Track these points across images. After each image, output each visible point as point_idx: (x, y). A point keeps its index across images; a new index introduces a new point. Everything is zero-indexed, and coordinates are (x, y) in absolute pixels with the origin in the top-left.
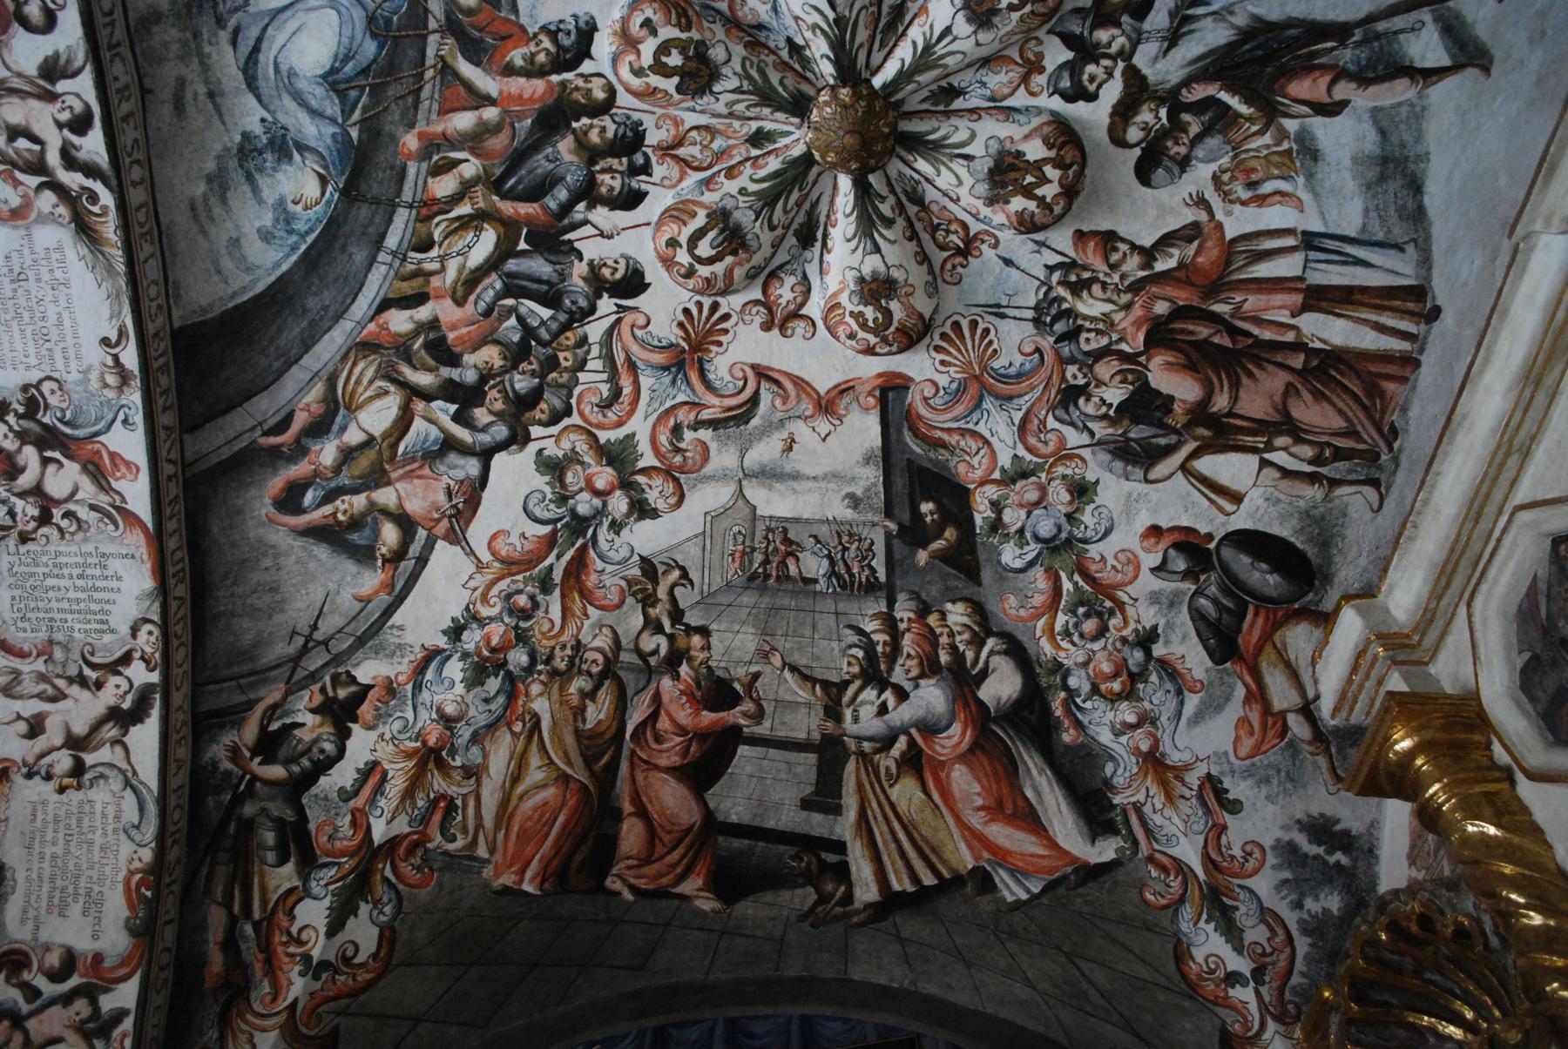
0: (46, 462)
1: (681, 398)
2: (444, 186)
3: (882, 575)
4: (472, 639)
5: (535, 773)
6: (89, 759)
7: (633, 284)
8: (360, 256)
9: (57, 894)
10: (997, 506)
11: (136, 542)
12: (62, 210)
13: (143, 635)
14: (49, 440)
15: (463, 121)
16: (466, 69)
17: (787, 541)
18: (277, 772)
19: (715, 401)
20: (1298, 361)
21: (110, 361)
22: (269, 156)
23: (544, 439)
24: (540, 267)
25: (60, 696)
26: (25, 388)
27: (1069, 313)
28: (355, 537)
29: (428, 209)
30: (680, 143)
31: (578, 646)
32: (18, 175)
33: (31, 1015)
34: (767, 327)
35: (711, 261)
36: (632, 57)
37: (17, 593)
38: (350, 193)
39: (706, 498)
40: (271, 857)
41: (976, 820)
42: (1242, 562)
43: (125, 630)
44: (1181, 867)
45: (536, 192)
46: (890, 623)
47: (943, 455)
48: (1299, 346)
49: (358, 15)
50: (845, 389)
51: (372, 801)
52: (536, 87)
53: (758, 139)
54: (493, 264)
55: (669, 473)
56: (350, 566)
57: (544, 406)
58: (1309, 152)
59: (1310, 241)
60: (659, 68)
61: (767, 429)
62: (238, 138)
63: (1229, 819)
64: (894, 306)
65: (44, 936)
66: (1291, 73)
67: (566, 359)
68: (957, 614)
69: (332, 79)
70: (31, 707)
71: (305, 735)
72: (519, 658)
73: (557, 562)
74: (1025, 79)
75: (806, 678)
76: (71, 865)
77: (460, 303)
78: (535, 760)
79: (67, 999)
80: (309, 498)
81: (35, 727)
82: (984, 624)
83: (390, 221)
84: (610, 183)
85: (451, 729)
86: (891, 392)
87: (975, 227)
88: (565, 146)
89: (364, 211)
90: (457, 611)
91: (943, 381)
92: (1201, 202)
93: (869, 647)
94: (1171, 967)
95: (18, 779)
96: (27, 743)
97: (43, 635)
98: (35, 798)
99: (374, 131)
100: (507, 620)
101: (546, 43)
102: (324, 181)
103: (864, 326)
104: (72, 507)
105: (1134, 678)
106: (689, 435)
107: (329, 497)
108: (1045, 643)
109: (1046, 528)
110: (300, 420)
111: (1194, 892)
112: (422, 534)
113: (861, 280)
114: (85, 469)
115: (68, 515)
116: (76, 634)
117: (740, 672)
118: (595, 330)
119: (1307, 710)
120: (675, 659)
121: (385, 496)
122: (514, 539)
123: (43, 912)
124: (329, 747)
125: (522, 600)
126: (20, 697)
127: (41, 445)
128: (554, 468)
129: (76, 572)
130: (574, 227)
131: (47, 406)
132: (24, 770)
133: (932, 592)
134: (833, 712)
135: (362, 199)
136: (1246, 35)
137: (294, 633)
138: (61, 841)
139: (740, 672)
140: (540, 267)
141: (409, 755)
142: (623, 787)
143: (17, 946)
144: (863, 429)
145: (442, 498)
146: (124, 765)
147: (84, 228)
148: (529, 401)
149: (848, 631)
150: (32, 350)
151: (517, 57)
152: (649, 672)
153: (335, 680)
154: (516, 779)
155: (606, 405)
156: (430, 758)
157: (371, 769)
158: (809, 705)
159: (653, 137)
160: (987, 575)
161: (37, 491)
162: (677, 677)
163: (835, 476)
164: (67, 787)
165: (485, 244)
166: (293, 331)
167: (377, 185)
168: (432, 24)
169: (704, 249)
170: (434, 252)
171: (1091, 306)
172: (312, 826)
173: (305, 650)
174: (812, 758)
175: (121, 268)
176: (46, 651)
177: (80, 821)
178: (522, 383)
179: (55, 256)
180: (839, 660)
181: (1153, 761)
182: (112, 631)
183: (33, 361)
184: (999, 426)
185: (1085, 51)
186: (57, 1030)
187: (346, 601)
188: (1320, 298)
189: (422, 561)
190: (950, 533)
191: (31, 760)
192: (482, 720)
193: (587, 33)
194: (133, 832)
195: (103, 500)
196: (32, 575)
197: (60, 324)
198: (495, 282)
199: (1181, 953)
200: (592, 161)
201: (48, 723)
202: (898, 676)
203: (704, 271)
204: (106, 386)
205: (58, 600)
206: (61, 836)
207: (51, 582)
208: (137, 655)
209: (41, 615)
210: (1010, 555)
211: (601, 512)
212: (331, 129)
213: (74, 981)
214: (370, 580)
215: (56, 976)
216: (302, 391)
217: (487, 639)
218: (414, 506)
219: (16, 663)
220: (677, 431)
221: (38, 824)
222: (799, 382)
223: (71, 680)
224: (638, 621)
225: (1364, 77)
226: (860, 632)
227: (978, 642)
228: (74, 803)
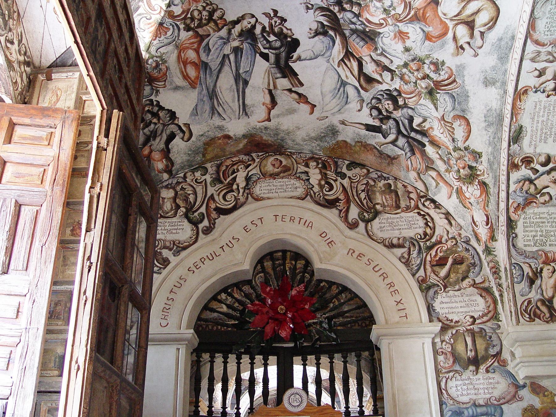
9: (543, 135)
33: (536, 179)
65: (538, 151)
70: (540, 66)
76: (549, 124)
79: (549, 172)
81: (541, 73)
95: (531, 93)
98: (537, 100)
123: (538, 142)
126: (538, 62)
132: (534, 90)
138: (546, 115)
143: (528, 155)
164: (550, 95)
186: (546, 184)
191: (537, 86)
201: (547, 71)
206: (546, 114)
213: (551, 165)
215: (544, 165)
219: (540, 48)
221: (537, 110)
228: (553, 101)
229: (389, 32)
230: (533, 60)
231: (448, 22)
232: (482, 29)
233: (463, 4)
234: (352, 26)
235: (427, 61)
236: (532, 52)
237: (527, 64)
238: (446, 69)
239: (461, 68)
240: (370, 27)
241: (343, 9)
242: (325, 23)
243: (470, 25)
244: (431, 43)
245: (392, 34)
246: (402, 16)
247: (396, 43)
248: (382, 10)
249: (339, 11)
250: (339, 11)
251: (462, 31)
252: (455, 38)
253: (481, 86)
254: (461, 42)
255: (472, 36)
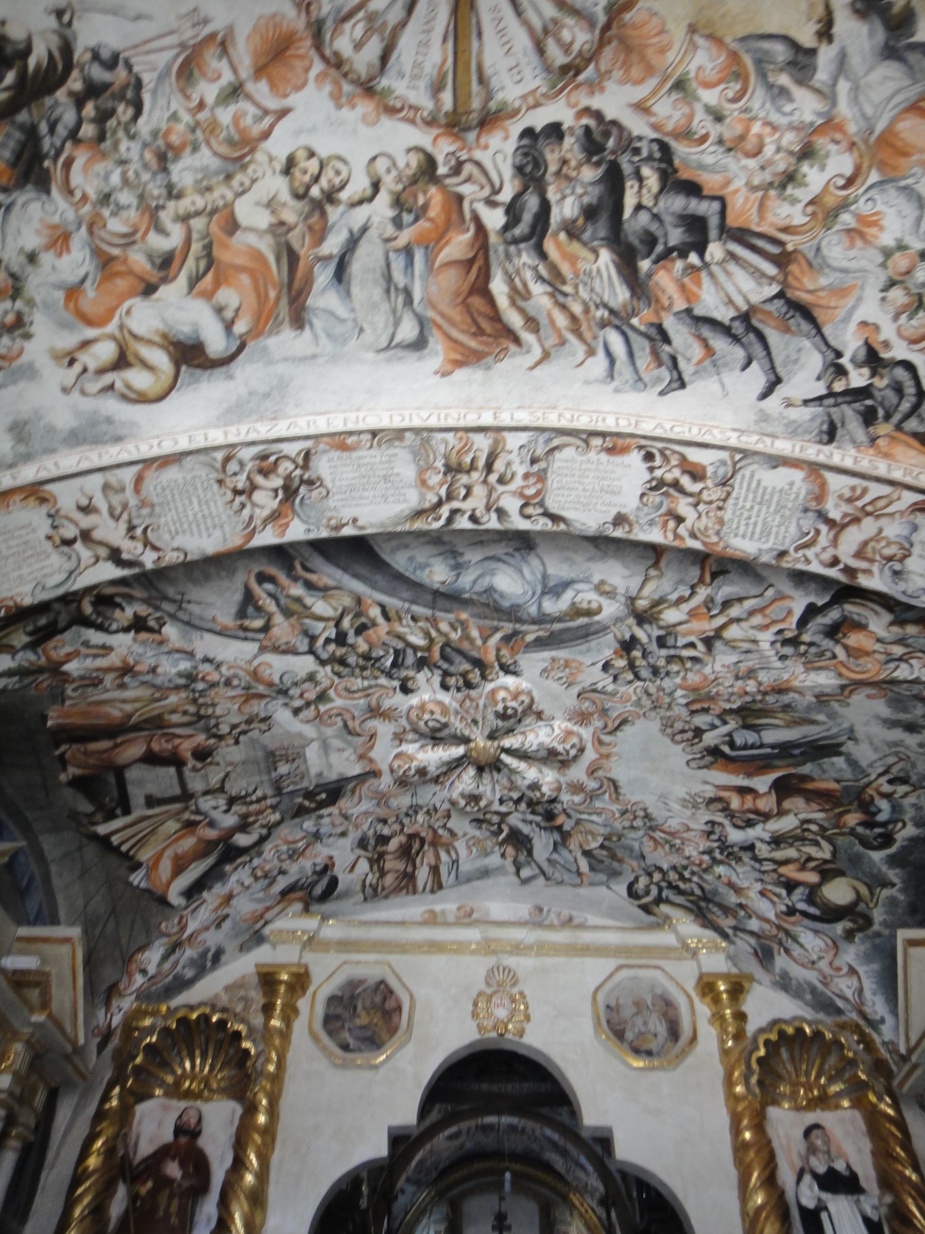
0: (276, 491)
1: (356, 714)
2: (444, 627)
3: (285, 791)
4: (206, 668)
5: (128, 708)
6: (78, 546)
7: (406, 689)
8: (406, 595)
10: (330, 815)
11: (235, 541)
12: (427, 505)
13: (175, 554)
14: (289, 492)
15: (475, 633)
16: (498, 636)
17: (294, 760)
18: (88, 609)
19: (357, 723)
20: (410, 869)
21: (344, 521)
22: (452, 562)
23: (325, 674)
24: (410, 659)
25: (117, 519)
26: (319, 479)
27: (416, 813)
28: (250, 610)
29: (434, 622)
30: (472, 700)
31: (214, 705)
32: (445, 487)
34: (395, 734)
35: (426, 723)
36: (509, 698)
37: (181, 481)
38: (436, 594)
39: (309, 731)
40: (30, 628)
41: (169, 853)
42: (325, 881)
43: (176, 544)
44: (183, 928)
45: (444, 656)
46: (264, 798)
47: (348, 794)
48: (415, 868)
49: (521, 601)
50: (371, 761)
51: (87, 656)
52: (491, 657)
53: (475, 722)
54: (409, 644)
55: (318, 715)
56: (233, 610)
57: (341, 669)
58: (487, 855)
59: (455, 862)
60: (506, 708)
61: (346, 741)
62: (461, 550)
63: (213, 928)
64: (417, 777)
66: (515, 847)
67: (367, 673)
68: (276, 817)
69: (490, 590)
70: (103, 506)
71: (118, 613)
72: (200, 686)
73: (261, 689)
74: (505, 788)
75: (223, 781)
77: (388, 633)
78: (137, 705)
80: (269, 586)
81: (86, 510)
82: (271, 828)
83: (425, 606)
84: (452, 681)
85: (148, 672)
86: (375, 774)
87: (448, 784)
88: (466, 666)
89: (429, 597)
90: (219, 658)
91: (382, 786)
92: (465, 835)
93: (247, 795)
94: (133, 950)
95: (44, 509)
96: (74, 507)
97: (155, 500)
99: (466, 603)
100: (223, 679)
101: (510, 662)
102: (444, 583)
103: (405, 772)
104: (249, 506)
105: (266, 876)
106: (339, 719)
107: (272, 595)
108: (270, 847)
109: (323, 830)
110: (313, 577)
111: (174, 938)
112: (261, 636)
113: (425, 768)
114: (274, 512)
115: (243, 506)
116: (163, 520)
117: (218, 759)
118: (383, 681)
119: (266, 923)
120: (221, 738)
121: (278, 619)
122: (268, 672)
124: (114, 626)
125: (235, 682)
127: (286, 488)
128: (311, 678)
129: (206, 512)
130: (431, 670)
131: (311, 491)
132: (53, 512)
133: (283, 807)
134: (206, 793)
135: (435, 598)
136: (527, 837)
137: (183, 595)
139: (218, 759)
140: (410, 659)
141: (124, 661)
142: (133, 735)
144: (356, 769)
145: (284, 640)
146: (82, 566)
147: (418, 513)
148: (342, 662)
149: (253, 788)
150: (344, 483)
151: (505, 652)
152: (207, 730)
153: (158, 619)
154: (124, 701)
155: (347, 689)
156: (126, 670)
157: (107, 649)
158: (208, 784)
159: (473, 693)
160: (297, 820)
161: (253, 487)
162: (207, 739)
163: (330, 766)
165: (417, 640)
166: (363, 571)
167: (441, 602)
168: (517, 626)
169: (431, 724)
170: (411, 623)
171: (420, 818)
172: (59, 637)
173: (173, 601)
174: (177, 791)
175: (399, 529)
176: (143, 504)
177: (32, 556)
178: (352, 660)
179: (402, 498)
180: (235, 787)
181: (230, 897)
182: (173, 538)
183: (337, 483)
184: (365, 806)
185: (518, 802)
187: (210, 613)
188: (435, 870)
189: (246, 639)
190: (313, 805)
191: (62, 513)
192: (158, 681)
193: (515, 673)
194: (39, 588)
195: (257, 522)
196: (196, 488)
197: (362, 498)
198: (400, 645)
199: (142, 948)
200: (461, 675)
202: (235, 808)
203: (422, 723)
204: (330, 519)
205: (184, 505)
207: (195, 501)
208: (161, 553)
209: (169, 497)
210: (309, 824)
211: (292, 698)
212: (468, 587)
214: (226, 618)
216: (329, 576)
217: (208, 674)
218: (275, 631)
220: (338, 715)
222: (372, 747)
223: (130, 521)
224: (236, 720)
225: (515, 862)
226: (254, 791)
227: (263, 826)
229: (59, 212)
230: (106, 487)
231: (115, 321)
232: (119, 385)
233: (157, 339)
234: (43, 128)
235: (19, 304)
236: (119, 481)
237: (97, 480)
238: (16, 348)
239: (31, 372)
240: (55, 169)
241: (79, 101)
242: (32, 62)
243: (122, 362)
244: (62, 302)
245: (56, 219)
246: (102, 233)
247: (38, 232)
248: (106, 190)
249: (71, 94)
250: (71, 94)
251: (106, 351)
252: (86, 344)
253: (8, 421)
254: (84, 359)
255: (101, 371)
